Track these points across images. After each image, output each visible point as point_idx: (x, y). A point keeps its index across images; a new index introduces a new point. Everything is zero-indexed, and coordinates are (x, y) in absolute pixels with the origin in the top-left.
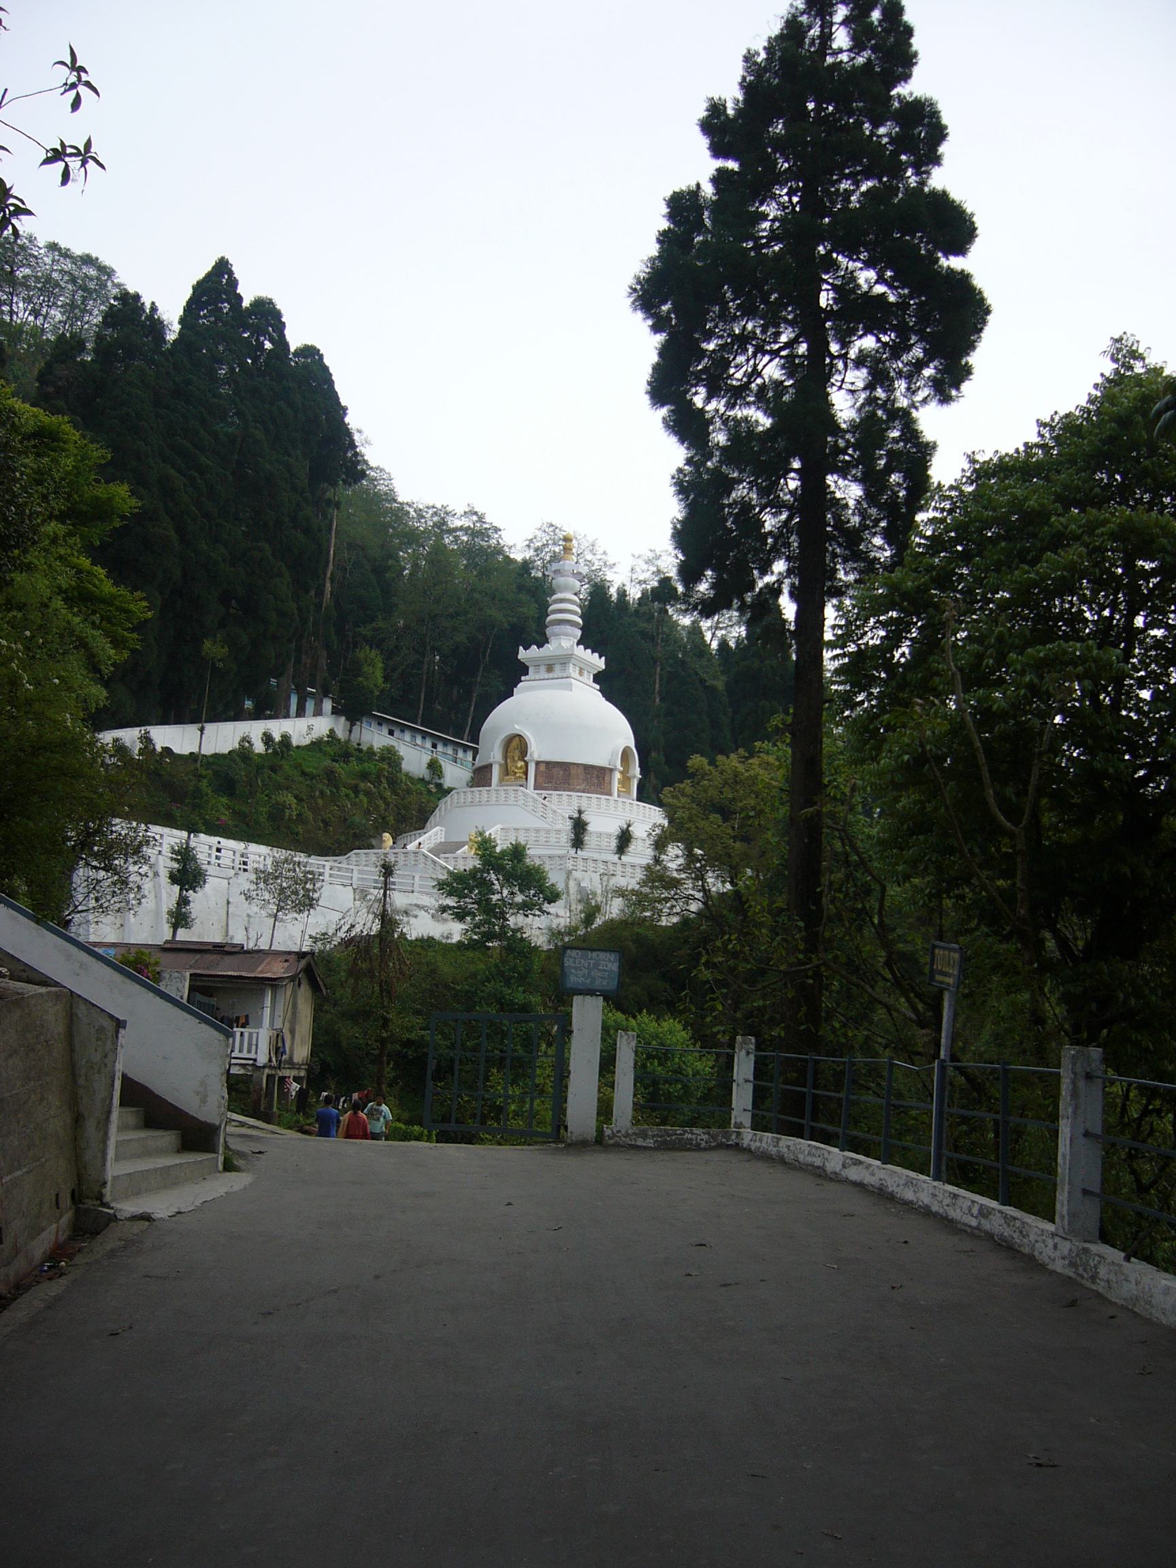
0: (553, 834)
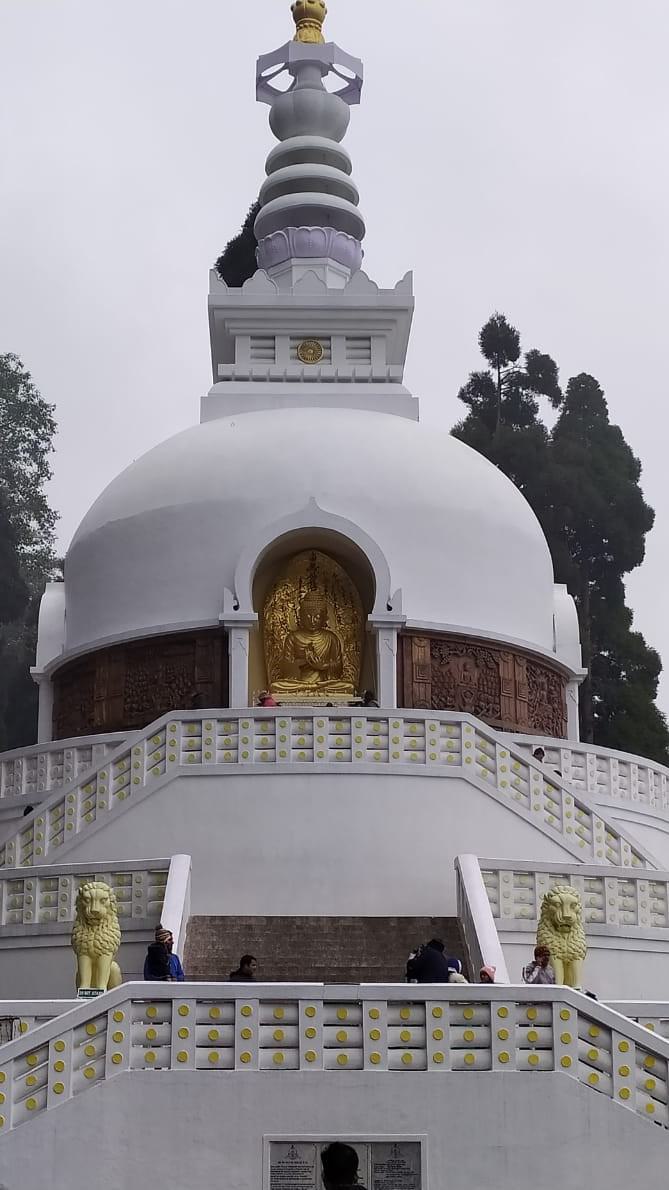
0: (613, 890)
